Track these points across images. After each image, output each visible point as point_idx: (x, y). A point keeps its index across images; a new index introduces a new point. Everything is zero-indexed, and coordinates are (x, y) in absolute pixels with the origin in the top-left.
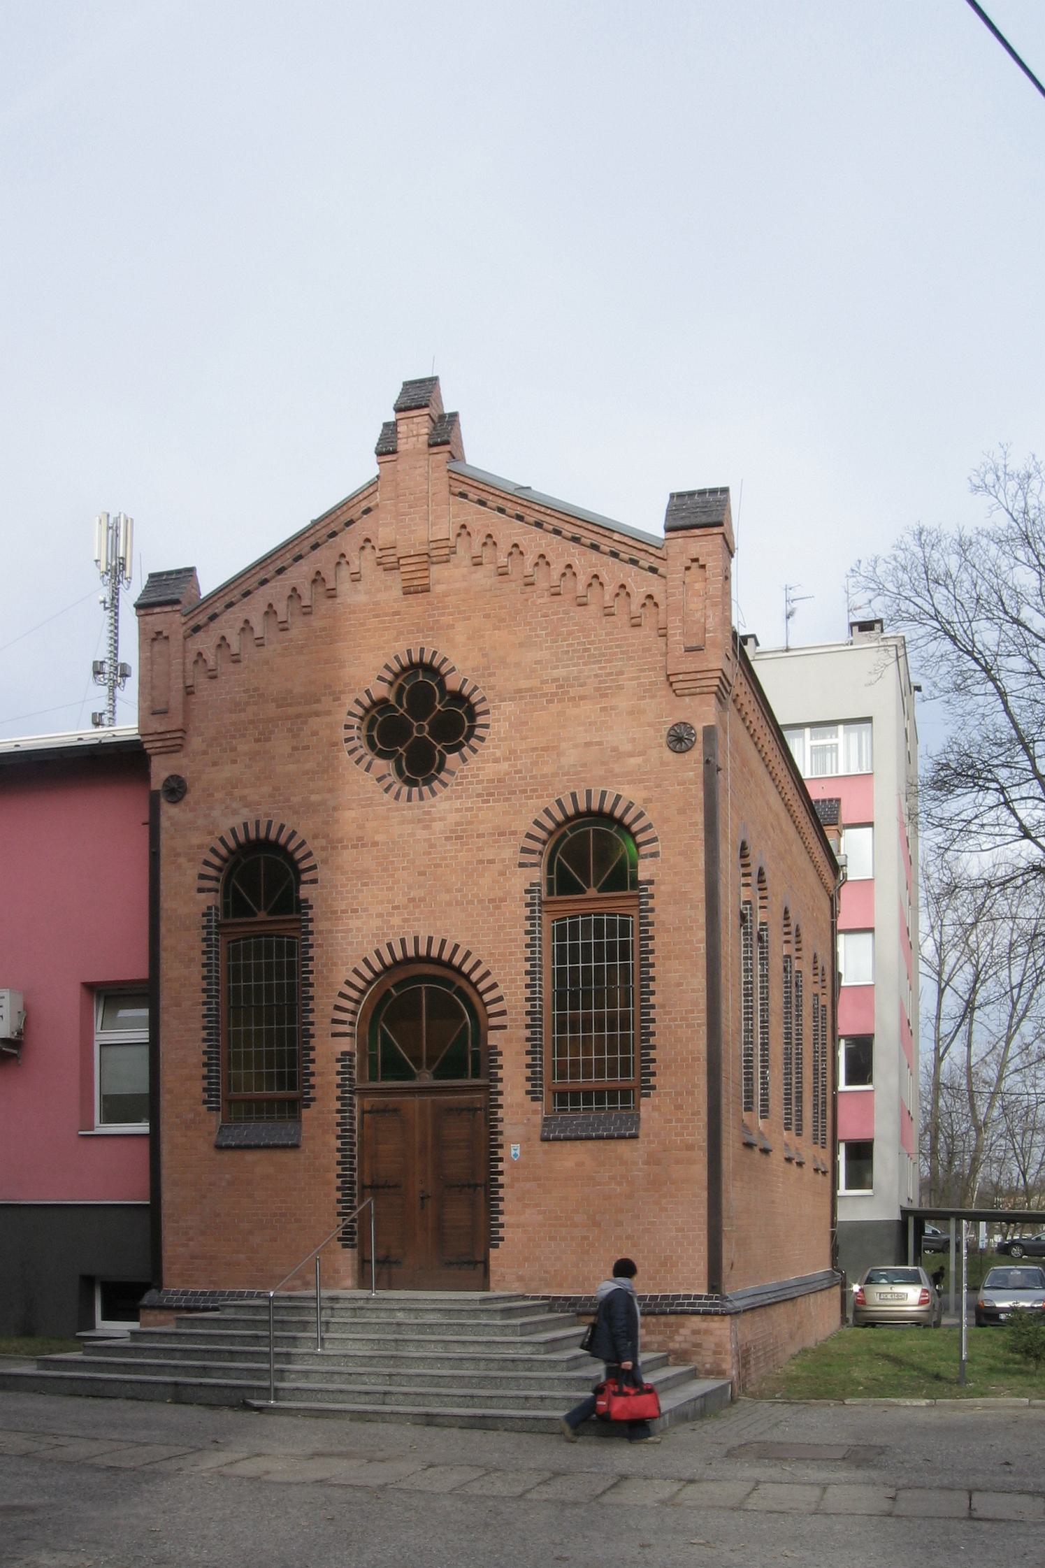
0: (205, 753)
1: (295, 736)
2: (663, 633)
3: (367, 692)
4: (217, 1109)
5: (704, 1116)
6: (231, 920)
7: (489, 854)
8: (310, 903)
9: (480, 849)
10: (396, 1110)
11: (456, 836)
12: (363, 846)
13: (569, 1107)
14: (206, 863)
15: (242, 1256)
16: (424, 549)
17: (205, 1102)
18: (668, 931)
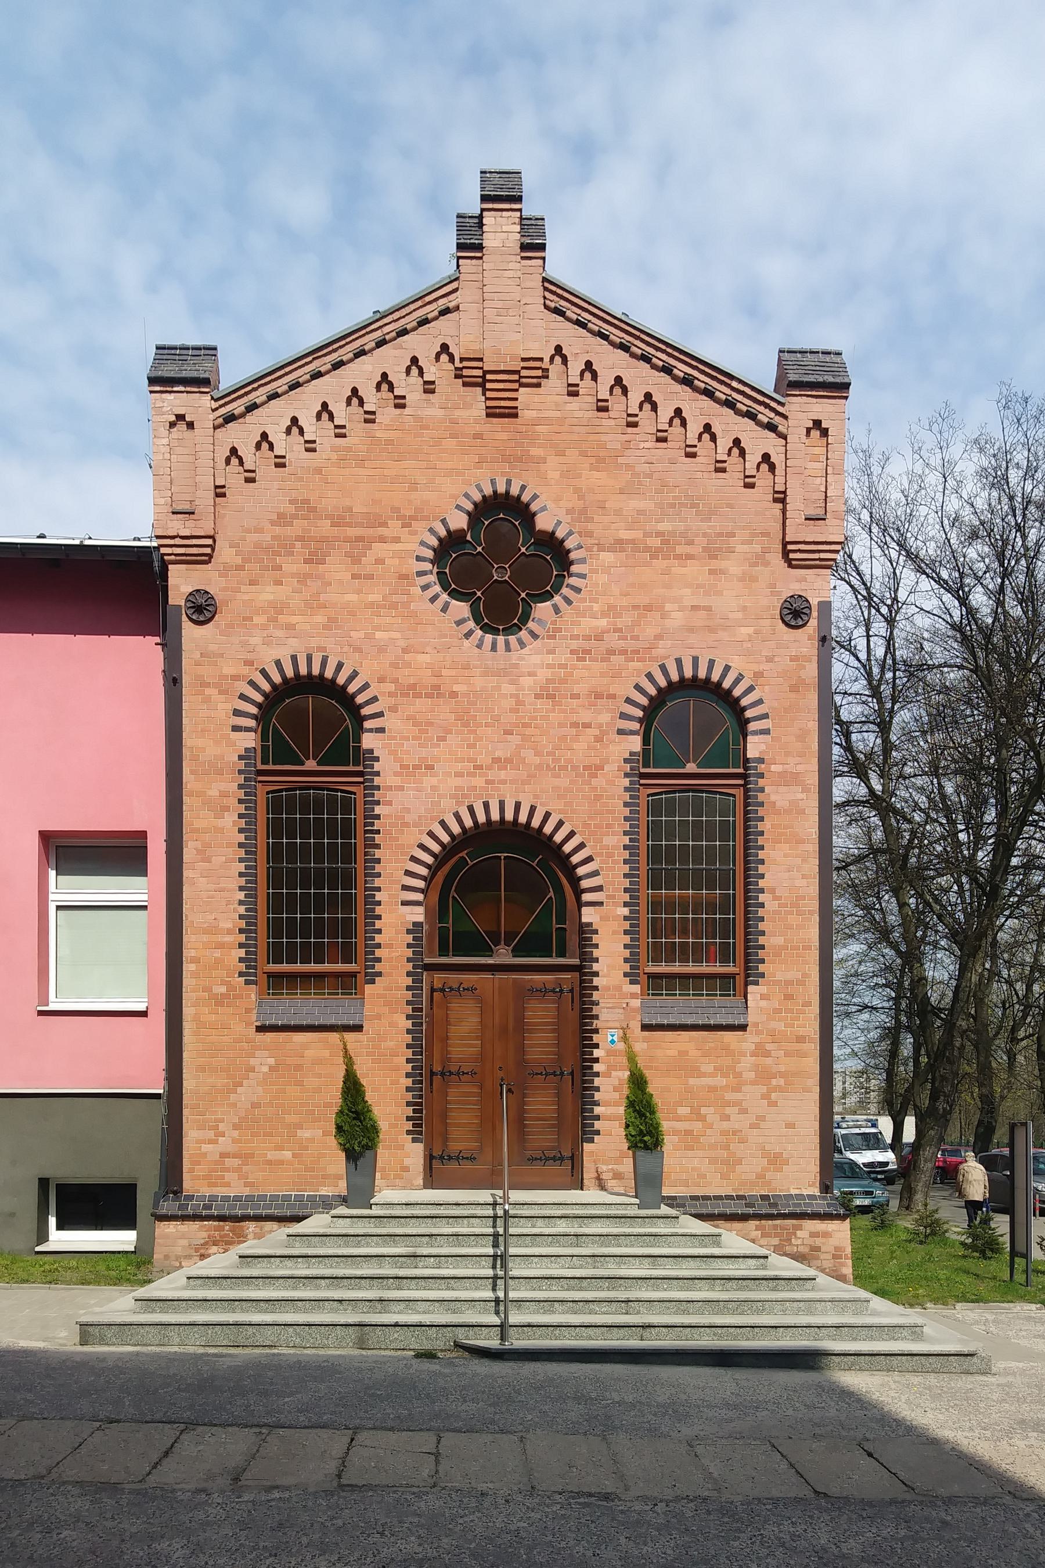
0: (240, 568)
1: (356, 561)
2: (781, 498)
3: (444, 521)
4: (255, 983)
5: (815, 1009)
6: (271, 767)
7: (585, 716)
8: (375, 755)
9: (573, 711)
10: (473, 989)
11: (547, 694)
12: (439, 696)
13: (678, 992)
14: (243, 697)
15: (288, 1154)
16: (517, 365)
17: (241, 974)
18: (778, 813)
